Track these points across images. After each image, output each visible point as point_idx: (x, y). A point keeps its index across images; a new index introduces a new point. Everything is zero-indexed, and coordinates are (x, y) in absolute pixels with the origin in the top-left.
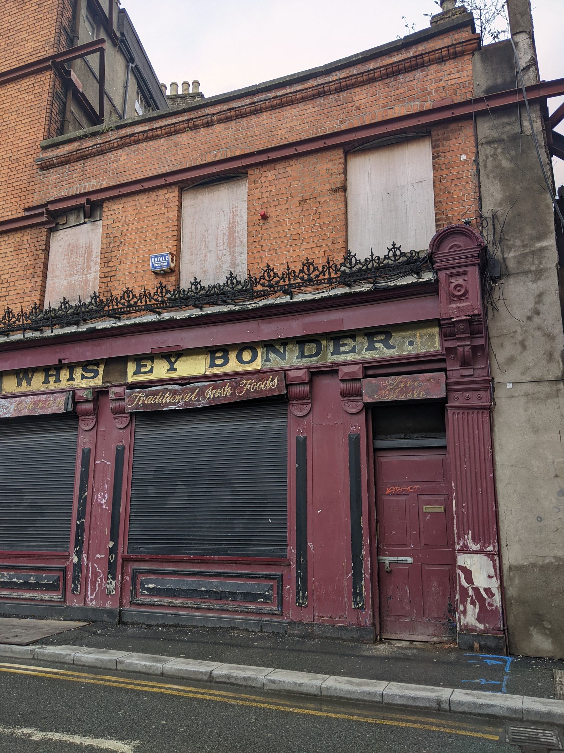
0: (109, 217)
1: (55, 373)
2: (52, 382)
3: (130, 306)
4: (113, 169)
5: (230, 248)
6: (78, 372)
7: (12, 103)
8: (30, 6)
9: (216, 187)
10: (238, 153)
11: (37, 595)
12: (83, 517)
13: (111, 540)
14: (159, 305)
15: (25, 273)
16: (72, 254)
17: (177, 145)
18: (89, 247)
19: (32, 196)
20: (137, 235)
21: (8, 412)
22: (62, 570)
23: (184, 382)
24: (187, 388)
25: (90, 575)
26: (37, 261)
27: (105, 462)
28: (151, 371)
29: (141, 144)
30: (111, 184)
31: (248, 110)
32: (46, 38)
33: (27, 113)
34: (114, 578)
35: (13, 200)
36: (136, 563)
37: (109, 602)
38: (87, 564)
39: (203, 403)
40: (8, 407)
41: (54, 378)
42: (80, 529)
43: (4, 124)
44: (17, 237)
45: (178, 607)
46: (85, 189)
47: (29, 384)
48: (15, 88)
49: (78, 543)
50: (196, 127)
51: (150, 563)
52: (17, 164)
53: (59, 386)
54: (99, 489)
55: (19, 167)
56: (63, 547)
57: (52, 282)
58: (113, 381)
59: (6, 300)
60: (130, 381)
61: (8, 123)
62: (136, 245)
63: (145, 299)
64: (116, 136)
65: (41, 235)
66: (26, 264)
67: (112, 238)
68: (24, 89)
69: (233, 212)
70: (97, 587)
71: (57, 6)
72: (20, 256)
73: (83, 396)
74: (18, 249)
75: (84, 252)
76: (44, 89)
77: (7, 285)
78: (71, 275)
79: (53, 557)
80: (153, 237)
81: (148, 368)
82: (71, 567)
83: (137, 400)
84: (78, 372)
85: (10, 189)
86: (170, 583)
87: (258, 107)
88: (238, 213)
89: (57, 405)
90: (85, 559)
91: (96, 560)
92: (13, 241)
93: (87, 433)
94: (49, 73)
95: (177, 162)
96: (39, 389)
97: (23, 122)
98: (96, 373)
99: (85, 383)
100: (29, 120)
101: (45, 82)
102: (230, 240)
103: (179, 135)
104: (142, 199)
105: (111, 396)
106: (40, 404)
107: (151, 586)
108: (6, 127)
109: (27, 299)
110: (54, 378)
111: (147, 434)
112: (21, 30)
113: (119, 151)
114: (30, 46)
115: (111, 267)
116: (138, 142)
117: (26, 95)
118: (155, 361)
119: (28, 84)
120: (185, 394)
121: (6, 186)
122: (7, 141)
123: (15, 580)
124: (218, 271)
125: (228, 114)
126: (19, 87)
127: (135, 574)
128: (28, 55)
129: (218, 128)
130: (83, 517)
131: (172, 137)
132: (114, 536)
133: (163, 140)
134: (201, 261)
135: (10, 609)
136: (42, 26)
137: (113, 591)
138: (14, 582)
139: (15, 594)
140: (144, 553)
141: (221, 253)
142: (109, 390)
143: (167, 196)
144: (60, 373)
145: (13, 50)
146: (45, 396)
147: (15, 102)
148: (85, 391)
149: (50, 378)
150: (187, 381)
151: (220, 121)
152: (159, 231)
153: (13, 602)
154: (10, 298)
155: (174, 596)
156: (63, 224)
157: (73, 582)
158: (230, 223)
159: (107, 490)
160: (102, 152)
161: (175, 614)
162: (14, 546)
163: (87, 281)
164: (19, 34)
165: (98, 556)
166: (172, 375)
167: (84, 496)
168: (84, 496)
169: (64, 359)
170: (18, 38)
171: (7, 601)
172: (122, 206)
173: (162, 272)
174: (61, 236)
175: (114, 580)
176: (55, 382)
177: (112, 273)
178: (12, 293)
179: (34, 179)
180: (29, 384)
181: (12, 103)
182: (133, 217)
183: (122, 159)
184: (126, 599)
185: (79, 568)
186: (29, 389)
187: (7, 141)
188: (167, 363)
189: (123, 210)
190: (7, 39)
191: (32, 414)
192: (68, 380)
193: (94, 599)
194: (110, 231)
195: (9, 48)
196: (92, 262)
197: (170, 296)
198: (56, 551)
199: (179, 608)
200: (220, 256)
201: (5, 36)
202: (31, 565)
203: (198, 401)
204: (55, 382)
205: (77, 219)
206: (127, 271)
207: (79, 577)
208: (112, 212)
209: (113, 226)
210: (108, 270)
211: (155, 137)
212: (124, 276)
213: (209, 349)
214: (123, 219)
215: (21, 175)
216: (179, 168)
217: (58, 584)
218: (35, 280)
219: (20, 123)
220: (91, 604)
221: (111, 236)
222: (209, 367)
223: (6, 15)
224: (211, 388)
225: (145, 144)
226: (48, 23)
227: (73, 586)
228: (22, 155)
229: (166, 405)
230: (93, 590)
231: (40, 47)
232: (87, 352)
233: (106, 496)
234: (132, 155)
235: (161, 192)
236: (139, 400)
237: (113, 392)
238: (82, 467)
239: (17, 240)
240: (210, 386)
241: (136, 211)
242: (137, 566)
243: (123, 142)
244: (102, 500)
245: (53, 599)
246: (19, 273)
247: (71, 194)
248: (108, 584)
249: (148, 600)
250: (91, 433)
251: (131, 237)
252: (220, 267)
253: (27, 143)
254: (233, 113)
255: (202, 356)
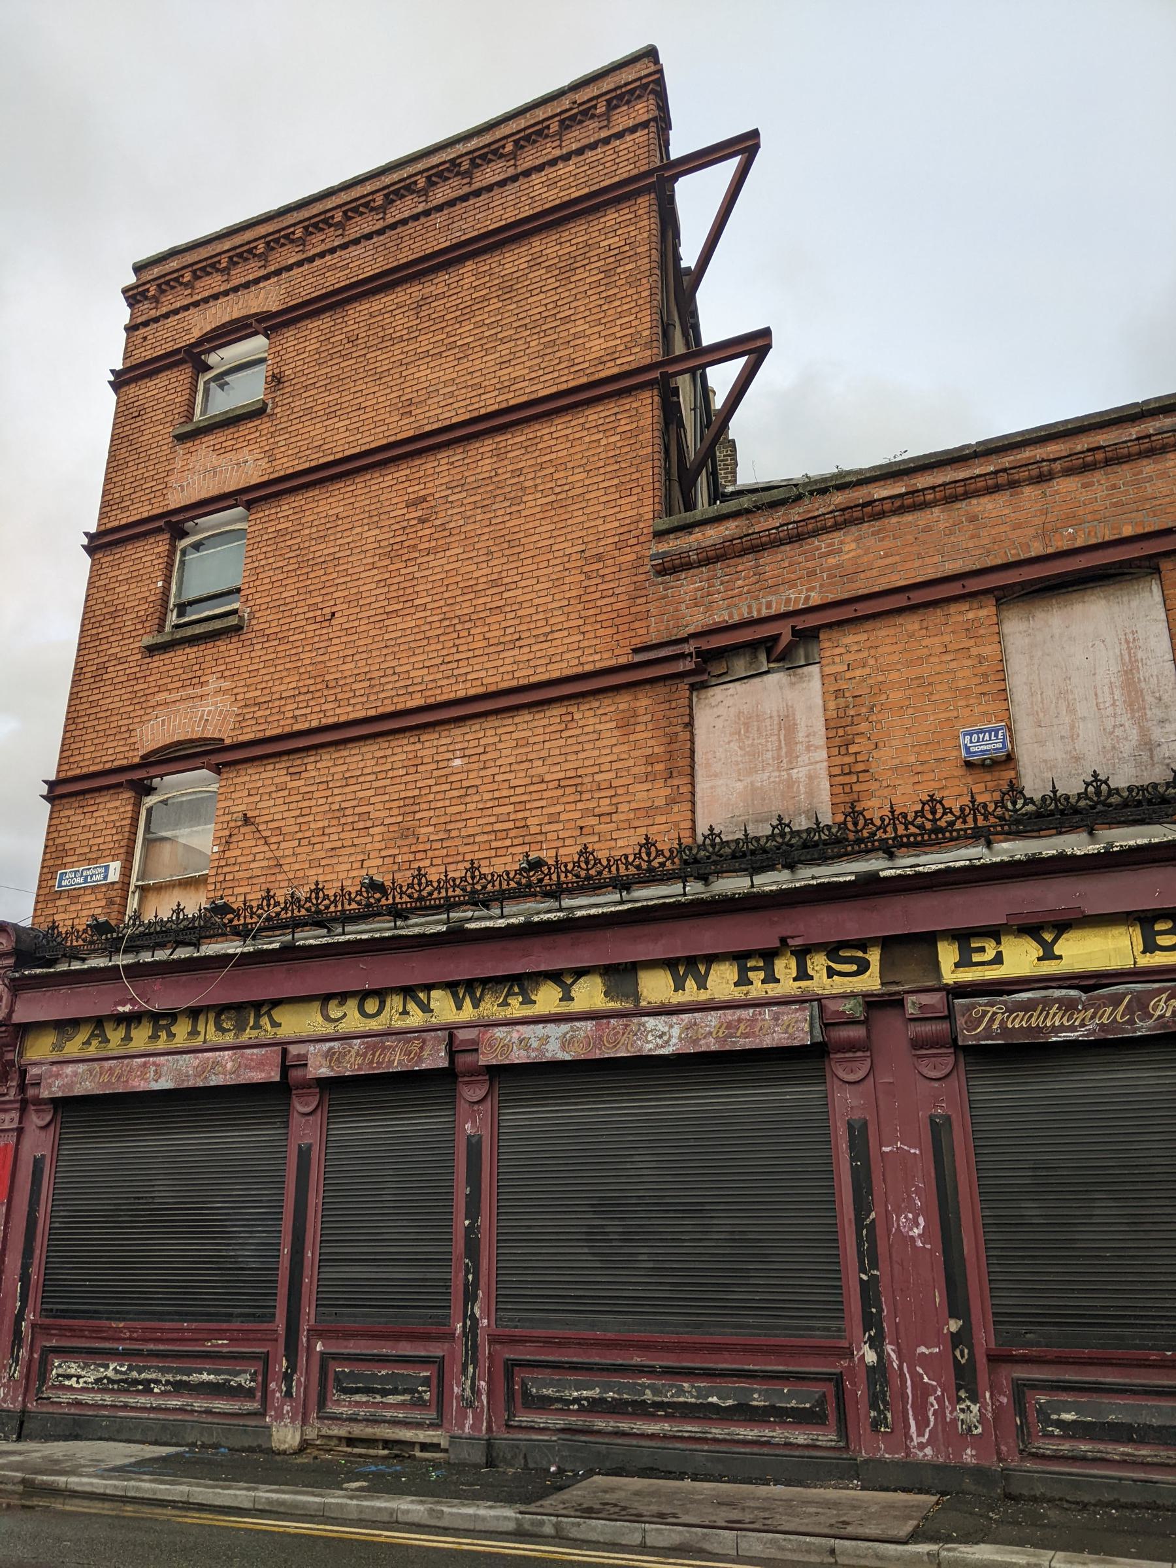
0: (837, 659)
1: (761, 964)
2: (758, 983)
3: (937, 830)
4: (830, 568)
5: (1132, 710)
6: (818, 963)
7: (572, 451)
8: (587, 274)
9: (1075, 595)
10: (1128, 531)
11: (777, 1434)
12: (874, 1265)
13: (953, 1315)
14: (1006, 828)
15: (649, 769)
16: (747, 731)
17: (973, 519)
18: (787, 716)
19: (644, 623)
20: (910, 692)
21: (667, 1042)
22: (830, 1380)
23: (1091, 982)
24: (1103, 997)
25: (909, 1391)
26: (675, 746)
27: (902, 1147)
28: (998, 960)
29: (886, 521)
30: (831, 597)
31: (1135, 450)
32: (632, 330)
33: (609, 469)
34: (974, 1398)
35: (600, 633)
36: (1018, 1367)
37: (969, 1451)
38: (900, 1367)
39: (1143, 1028)
40: (664, 1033)
41: (762, 975)
42: (869, 1291)
43: (557, 490)
44: (623, 702)
45: (1148, 1464)
46: (769, 606)
47: (702, 985)
48: (573, 423)
49: (871, 1321)
50: (1013, 485)
51: (1053, 1368)
52: (600, 565)
53: (774, 990)
54: (900, 1207)
55: (606, 571)
56: (828, 1329)
57: (709, 784)
58: (907, 982)
59: (611, 822)
60: (951, 982)
61: (566, 488)
62: (910, 711)
63: (975, 815)
64: (832, 507)
65: (676, 696)
66: (649, 751)
67: (850, 699)
68: (594, 424)
69: (1127, 642)
70: (932, 1419)
71: (648, 273)
72: (632, 737)
73: (844, 1012)
74: (626, 724)
75: (776, 727)
76: (641, 423)
77: (612, 792)
78: (752, 771)
79: (808, 1351)
80: (948, 695)
81: (990, 954)
82: (862, 1375)
83: (986, 1019)
84: (818, 963)
85: (591, 612)
86: (1116, 1411)
87: (1158, 444)
88: (1141, 643)
89: (792, 1029)
90: (893, 1356)
91: (915, 1359)
92: (612, 709)
93: (853, 1087)
94: (648, 394)
95: (982, 551)
96: (730, 997)
97: (602, 485)
98: (864, 967)
99: (841, 985)
100: (616, 481)
101: (644, 409)
102: (1129, 695)
103: (974, 501)
104: (911, 623)
105: (911, 1011)
106: (742, 1026)
107: (1069, 1417)
108: (563, 496)
109: (661, 819)
110: (762, 975)
111: (1005, 1091)
112: (573, 318)
113: (835, 534)
114: (597, 347)
115: (856, 753)
116: (882, 515)
117: (601, 435)
118: (1004, 939)
119: (603, 414)
120: (1099, 1007)
121: (580, 607)
122: (569, 522)
123: (714, 1399)
124: (1109, 756)
125: (1090, 459)
126: (582, 420)
127: (1020, 1390)
128: (593, 363)
129: (1066, 486)
130: (874, 1265)
131: (958, 505)
132: (957, 1306)
133: (936, 510)
134: (1062, 737)
135: (709, 1464)
136: (619, 310)
137: (976, 1428)
138: (712, 1404)
139: (716, 1431)
140: (1038, 1344)
141: (1109, 724)
142: (902, 1000)
143: (971, 615)
144: (773, 964)
145: (558, 355)
146: (751, 1011)
147: (578, 449)
148: (846, 1001)
149: (751, 975)
150: (1092, 982)
151: (1069, 472)
152: (962, 683)
153: (712, 1448)
154: (622, 817)
155: (1131, 1440)
156: (720, 675)
157: (873, 1406)
158: (1123, 665)
159: (921, 1209)
160: (797, 538)
161: (1141, 1481)
162: (701, 1325)
163: (791, 783)
164: (568, 326)
165: (922, 1349)
166: (1050, 968)
167: (868, 1221)
168: (868, 1221)
169: (792, 937)
170: (566, 333)
171: (698, 1447)
172: (864, 636)
173: (988, 762)
174: (719, 697)
175: (974, 1402)
176: (763, 982)
177: (861, 767)
178: (623, 807)
179: (643, 592)
180: (702, 985)
181: (572, 451)
182: (896, 657)
183: (846, 548)
184: (1006, 1444)
185: (884, 1376)
186: (703, 996)
187: (569, 522)
188: (1035, 944)
189: (868, 644)
190: (542, 334)
191: (727, 1048)
192: (795, 980)
193: (929, 1443)
194: (842, 685)
195: (548, 351)
196: (799, 746)
197: (1034, 808)
198: (811, 1337)
199: (1148, 1468)
200: (1109, 728)
201: (538, 329)
202: (751, 1367)
203: (1131, 1022)
204: (763, 982)
205: (751, 664)
206: (897, 761)
207: (885, 1395)
208: (842, 650)
209: (849, 675)
210: (849, 760)
211: (921, 504)
212: (890, 772)
213: (1136, 915)
214: (871, 662)
215: (612, 585)
216: (990, 562)
217: (823, 1410)
218: (676, 782)
219: (595, 487)
220: (921, 1454)
221: (847, 695)
222: (1144, 952)
223: (534, 293)
224: (1164, 996)
225: (894, 520)
226: (633, 304)
227: (873, 1414)
228: (608, 548)
229: (1055, 1030)
230: (922, 1424)
231: (622, 347)
232: (847, 922)
233: (921, 1220)
234: (871, 542)
235: (953, 608)
236: (992, 1020)
237: (914, 1003)
238: (852, 1159)
239: (622, 707)
240: (1160, 992)
241: (900, 647)
242: (1021, 1373)
243: (847, 516)
244: (912, 1229)
245: (819, 1443)
246: (635, 770)
247: (736, 618)
248: (962, 1410)
249: (1066, 1447)
250: (861, 1087)
251: (896, 696)
252: (1114, 748)
253: (617, 524)
254: (1100, 456)
255: (1122, 929)
